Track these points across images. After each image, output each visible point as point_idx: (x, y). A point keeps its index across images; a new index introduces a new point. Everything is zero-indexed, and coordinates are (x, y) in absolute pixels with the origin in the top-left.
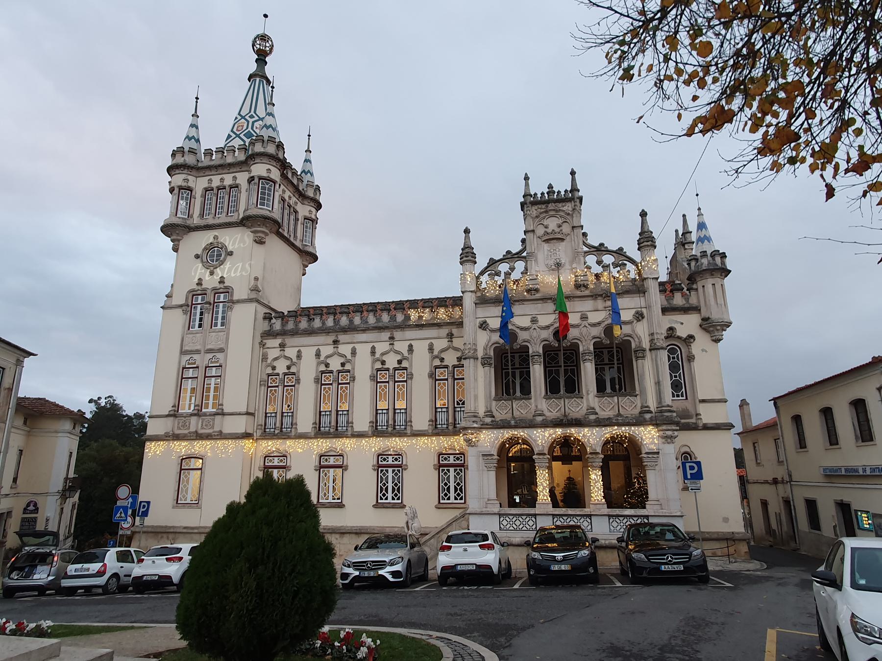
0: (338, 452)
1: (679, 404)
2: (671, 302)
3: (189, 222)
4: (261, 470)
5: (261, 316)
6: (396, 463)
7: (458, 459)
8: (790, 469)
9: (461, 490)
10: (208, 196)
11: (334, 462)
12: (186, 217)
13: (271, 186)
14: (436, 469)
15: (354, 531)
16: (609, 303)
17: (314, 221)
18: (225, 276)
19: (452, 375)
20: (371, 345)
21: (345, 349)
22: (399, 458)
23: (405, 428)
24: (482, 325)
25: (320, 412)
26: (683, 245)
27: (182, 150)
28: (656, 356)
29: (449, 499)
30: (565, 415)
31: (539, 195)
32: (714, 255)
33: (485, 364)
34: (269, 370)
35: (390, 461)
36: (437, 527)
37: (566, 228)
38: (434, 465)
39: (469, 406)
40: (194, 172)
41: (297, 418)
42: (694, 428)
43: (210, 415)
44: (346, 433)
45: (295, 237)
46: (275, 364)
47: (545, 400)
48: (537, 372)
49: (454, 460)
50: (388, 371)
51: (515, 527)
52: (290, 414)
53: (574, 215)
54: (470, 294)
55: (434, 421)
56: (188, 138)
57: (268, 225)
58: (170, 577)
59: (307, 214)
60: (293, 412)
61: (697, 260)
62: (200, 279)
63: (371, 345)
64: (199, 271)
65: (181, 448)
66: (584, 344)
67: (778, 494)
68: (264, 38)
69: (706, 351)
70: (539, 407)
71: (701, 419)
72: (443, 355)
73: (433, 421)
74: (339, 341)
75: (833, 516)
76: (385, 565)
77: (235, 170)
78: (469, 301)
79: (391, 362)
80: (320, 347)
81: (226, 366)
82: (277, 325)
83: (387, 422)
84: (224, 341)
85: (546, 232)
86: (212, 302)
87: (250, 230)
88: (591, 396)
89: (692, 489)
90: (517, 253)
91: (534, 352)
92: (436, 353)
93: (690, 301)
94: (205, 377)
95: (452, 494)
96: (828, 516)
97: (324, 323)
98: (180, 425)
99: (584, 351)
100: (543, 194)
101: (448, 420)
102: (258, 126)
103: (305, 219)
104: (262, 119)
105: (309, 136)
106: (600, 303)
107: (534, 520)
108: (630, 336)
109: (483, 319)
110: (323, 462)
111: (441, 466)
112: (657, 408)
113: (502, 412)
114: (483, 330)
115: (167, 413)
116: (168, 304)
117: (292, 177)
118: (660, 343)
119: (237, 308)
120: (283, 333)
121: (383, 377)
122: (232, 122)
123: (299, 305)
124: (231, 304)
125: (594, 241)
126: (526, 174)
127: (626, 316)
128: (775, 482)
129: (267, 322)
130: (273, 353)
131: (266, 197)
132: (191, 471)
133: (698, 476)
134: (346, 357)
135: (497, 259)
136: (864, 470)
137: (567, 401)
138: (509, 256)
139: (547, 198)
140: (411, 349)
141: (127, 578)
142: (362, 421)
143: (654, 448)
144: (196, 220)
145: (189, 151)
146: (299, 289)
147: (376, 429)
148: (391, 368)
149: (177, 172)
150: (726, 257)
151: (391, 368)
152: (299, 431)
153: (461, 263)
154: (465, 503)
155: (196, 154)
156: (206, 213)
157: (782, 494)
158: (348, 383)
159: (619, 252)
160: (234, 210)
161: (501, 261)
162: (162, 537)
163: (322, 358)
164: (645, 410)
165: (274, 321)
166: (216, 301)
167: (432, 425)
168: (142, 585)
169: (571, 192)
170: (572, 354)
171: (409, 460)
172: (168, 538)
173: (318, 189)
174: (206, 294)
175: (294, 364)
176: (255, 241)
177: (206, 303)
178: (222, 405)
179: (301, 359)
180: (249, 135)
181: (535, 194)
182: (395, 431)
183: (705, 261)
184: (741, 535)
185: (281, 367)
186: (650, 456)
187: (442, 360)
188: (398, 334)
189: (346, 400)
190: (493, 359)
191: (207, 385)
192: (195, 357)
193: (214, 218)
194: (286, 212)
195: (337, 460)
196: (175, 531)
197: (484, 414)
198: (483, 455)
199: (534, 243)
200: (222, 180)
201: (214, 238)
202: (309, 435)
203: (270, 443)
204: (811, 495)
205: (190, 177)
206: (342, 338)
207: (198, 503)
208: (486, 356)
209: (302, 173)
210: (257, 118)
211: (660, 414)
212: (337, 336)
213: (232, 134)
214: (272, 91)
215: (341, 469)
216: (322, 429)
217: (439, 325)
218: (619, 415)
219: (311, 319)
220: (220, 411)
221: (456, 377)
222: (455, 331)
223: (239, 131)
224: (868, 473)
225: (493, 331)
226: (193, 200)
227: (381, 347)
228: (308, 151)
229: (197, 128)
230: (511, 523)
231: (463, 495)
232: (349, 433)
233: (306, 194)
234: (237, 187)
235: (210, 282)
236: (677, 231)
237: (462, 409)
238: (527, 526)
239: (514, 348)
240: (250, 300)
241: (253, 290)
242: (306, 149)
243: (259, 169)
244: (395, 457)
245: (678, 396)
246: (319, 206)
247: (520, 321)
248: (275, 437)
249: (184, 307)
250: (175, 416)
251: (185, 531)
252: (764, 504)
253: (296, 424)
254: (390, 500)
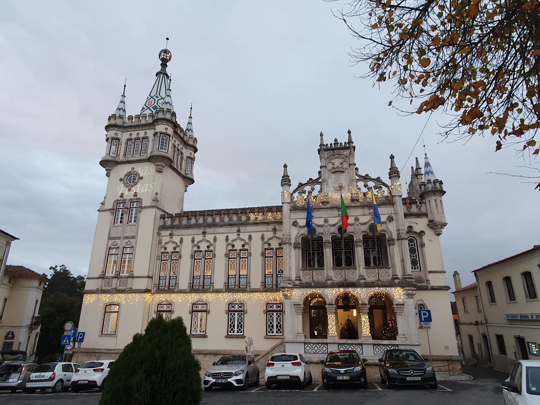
0: (204, 302)
1: (416, 274)
2: (410, 210)
3: (117, 159)
4: (155, 313)
5: (158, 216)
6: (240, 309)
7: (279, 307)
8: (486, 316)
9: (280, 326)
10: (129, 143)
11: (201, 308)
12: (116, 156)
13: (167, 138)
14: (265, 313)
15: (213, 353)
16: (372, 211)
17: (193, 159)
18: (137, 192)
19: (275, 254)
20: (226, 235)
21: (210, 237)
22: (242, 306)
23: (246, 287)
24: (294, 223)
25: (193, 276)
26: (417, 176)
27: (115, 116)
28: (401, 244)
29: (273, 332)
30: (345, 280)
31: (329, 145)
32: (436, 182)
33: (296, 248)
34: (163, 250)
35: (236, 308)
36: (265, 351)
37: (345, 165)
38: (264, 311)
39: (286, 274)
40: (121, 130)
41: (179, 280)
42: (425, 289)
43: (125, 278)
44: (209, 290)
45: (181, 168)
46: (166, 246)
47: (333, 270)
48: (328, 253)
49: (276, 308)
50: (236, 251)
51: (314, 351)
52: (175, 278)
53: (350, 157)
54: (287, 204)
55: (264, 283)
56: (119, 109)
57: (165, 161)
58: (95, 382)
59: (189, 155)
60: (176, 277)
61: (425, 185)
62: (122, 194)
63: (226, 235)
64: (122, 188)
65: (106, 298)
66: (357, 235)
67: (479, 332)
68: (166, 51)
69: (432, 241)
70: (329, 275)
71: (430, 283)
72: (270, 242)
73: (263, 283)
74: (206, 233)
75: (514, 346)
76: (232, 375)
77: (146, 128)
78: (286, 209)
79: (238, 245)
80: (194, 236)
81: (136, 247)
82: (169, 222)
83: (235, 283)
84: (136, 232)
85: (333, 167)
86: (129, 208)
87: (153, 164)
88: (361, 268)
89: (425, 328)
90: (316, 180)
91: (326, 240)
92: (265, 240)
93: (422, 210)
94: (123, 254)
95: (275, 329)
96: (511, 345)
97: (197, 221)
98: (106, 283)
99: (356, 240)
100: (331, 144)
101: (272, 282)
102: (161, 103)
103: (187, 158)
104: (163, 99)
105: (191, 108)
106: (366, 211)
107: (326, 347)
108: (384, 231)
109: (295, 220)
110: (194, 308)
111: (268, 311)
112: (402, 276)
113: (306, 278)
114: (295, 226)
115: (98, 276)
116: (102, 209)
117: (180, 132)
118: (403, 235)
119: (144, 211)
120: (172, 227)
121: (233, 255)
122: (146, 100)
123: (182, 210)
124: (141, 209)
125: (362, 173)
126: (321, 132)
127: (383, 218)
128: (477, 323)
129: (162, 220)
130: (165, 240)
131: (164, 144)
132: (112, 313)
133: (429, 319)
134: (210, 242)
135: (303, 183)
136: (532, 317)
137: (346, 271)
138: (311, 181)
139: (334, 147)
140: (250, 238)
141: (68, 382)
142: (219, 282)
143: (401, 301)
144: (121, 158)
145: (119, 117)
146: (182, 200)
147: (228, 287)
148: (238, 249)
149: (111, 129)
150: (443, 183)
151: (238, 249)
152: (180, 288)
153: (282, 186)
154: (283, 335)
155: (123, 118)
156: (128, 154)
157: (481, 331)
158: (211, 259)
159: (378, 180)
160: (144, 152)
161: (306, 184)
162: (91, 356)
163: (195, 243)
164: (395, 277)
165: (166, 219)
166: (131, 207)
167: (263, 285)
168: (78, 387)
169: (348, 143)
170: (350, 242)
171: (248, 308)
172: (95, 356)
173: (195, 140)
174: (125, 203)
175: (178, 246)
176: (157, 171)
177: (125, 208)
178: (133, 271)
179: (182, 243)
180: (155, 108)
181: (327, 144)
182: (239, 289)
183: (430, 186)
184: (456, 358)
185: (170, 248)
186: (398, 306)
187: (269, 245)
188: (242, 229)
189: (210, 269)
190: (301, 245)
191: (124, 259)
192: (117, 241)
193: (132, 157)
194: (176, 153)
195: (203, 307)
196: (100, 351)
197: (295, 279)
198: (295, 305)
199: (326, 174)
200: (138, 134)
201: (132, 169)
202: (186, 291)
203: (162, 296)
204: (499, 332)
205: (118, 132)
206: (208, 230)
207: (115, 334)
208: (297, 243)
209: (186, 130)
210: (160, 98)
211: (404, 280)
212: (205, 229)
213: (145, 107)
214: (170, 82)
215: (206, 313)
216: (194, 287)
217: (268, 223)
218: (379, 280)
219: (189, 219)
220: (131, 275)
221: (278, 255)
222: (277, 227)
223: (149, 105)
224: (535, 318)
225: (300, 227)
226: (120, 146)
227: (232, 237)
228: (190, 117)
229: (124, 103)
230: (312, 348)
231: (282, 330)
232: (211, 290)
233: (188, 143)
234: (147, 138)
235: (128, 195)
236: (412, 167)
237: (282, 275)
238: (322, 350)
239: (314, 238)
240: (152, 207)
241: (154, 201)
242: (189, 116)
243: (161, 128)
244: (240, 305)
245: (415, 268)
246: (196, 150)
247: (317, 221)
248: (165, 292)
249: (111, 211)
250: (103, 278)
251: (106, 351)
252: (471, 338)
253: (178, 284)
254: (236, 333)
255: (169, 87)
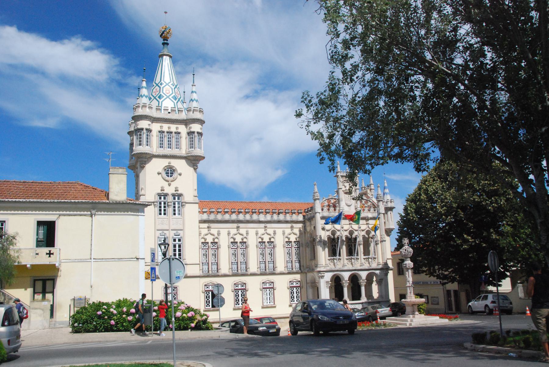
92: (286, 235)
95: (295, 299)
136: (431, 283)
163: (231, 235)
188: (268, 225)
192: (165, 232)
206: (241, 225)
223: (168, 94)
225: (328, 231)
226: (152, 137)
255: (194, 83)
